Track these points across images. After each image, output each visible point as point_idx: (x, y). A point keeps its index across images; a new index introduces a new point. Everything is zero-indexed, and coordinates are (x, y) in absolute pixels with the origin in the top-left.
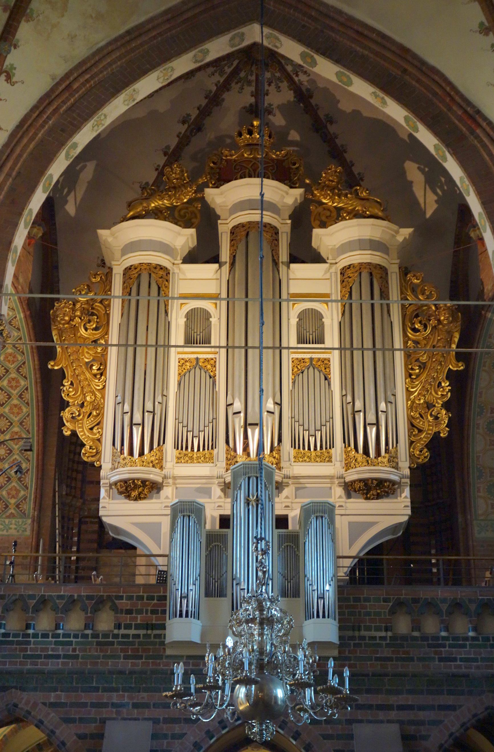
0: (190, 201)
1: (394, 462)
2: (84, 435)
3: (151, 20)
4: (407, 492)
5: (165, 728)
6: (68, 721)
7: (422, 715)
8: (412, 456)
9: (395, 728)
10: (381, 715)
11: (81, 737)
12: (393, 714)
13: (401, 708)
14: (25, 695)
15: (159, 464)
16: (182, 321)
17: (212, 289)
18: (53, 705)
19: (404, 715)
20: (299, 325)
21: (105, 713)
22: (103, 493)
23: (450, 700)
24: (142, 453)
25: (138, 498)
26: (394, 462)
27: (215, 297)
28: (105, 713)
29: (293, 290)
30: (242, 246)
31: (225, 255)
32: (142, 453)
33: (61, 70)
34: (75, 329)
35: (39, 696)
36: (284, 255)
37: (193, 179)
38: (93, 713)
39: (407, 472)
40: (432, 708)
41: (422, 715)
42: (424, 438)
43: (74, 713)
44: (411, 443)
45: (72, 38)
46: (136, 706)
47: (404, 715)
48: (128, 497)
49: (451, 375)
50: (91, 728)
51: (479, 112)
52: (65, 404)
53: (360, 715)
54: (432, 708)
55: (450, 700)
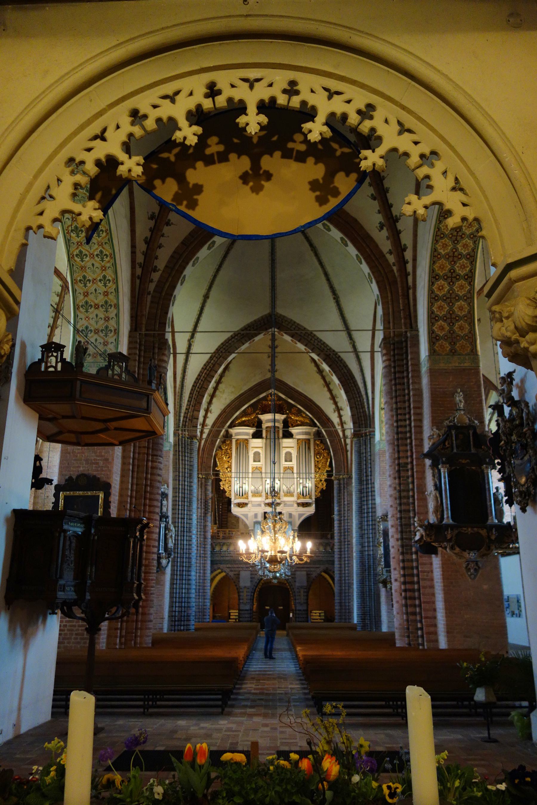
0: (254, 418)
1: (310, 498)
2: (226, 489)
3: (245, 391)
4: (314, 505)
5: (253, 573)
6: (232, 571)
7: (312, 569)
8: (316, 495)
9: (305, 573)
10: (302, 569)
11: (235, 575)
12: (305, 569)
13: (307, 568)
14: (222, 565)
15: (247, 498)
16: (252, 455)
17: (260, 445)
18: (228, 568)
19: (308, 569)
20: (285, 457)
21: (241, 569)
22: (232, 506)
23: (318, 566)
24: (242, 495)
25: (242, 507)
26: (310, 498)
27: (262, 447)
28: (241, 569)
29: (284, 446)
30: (269, 433)
31: (264, 435)
32: (242, 495)
33: (223, 407)
34: (223, 458)
35: (225, 566)
36: (281, 435)
37: (254, 412)
38: (237, 569)
39: (314, 500)
40: (313, 568)
41: (312, 569)
42: (319, 490)
43: (233, 569)
44: (316, 491)
45: (226, 399)
46: (247, 568)
47: (308, 569)
48: (239, 507)
49: (327, 471)
50: (236, 573)
51: (329, 418)
52: (221, 480)
53: (298, 569)
54: (313, 568)
55: (318, 566)
